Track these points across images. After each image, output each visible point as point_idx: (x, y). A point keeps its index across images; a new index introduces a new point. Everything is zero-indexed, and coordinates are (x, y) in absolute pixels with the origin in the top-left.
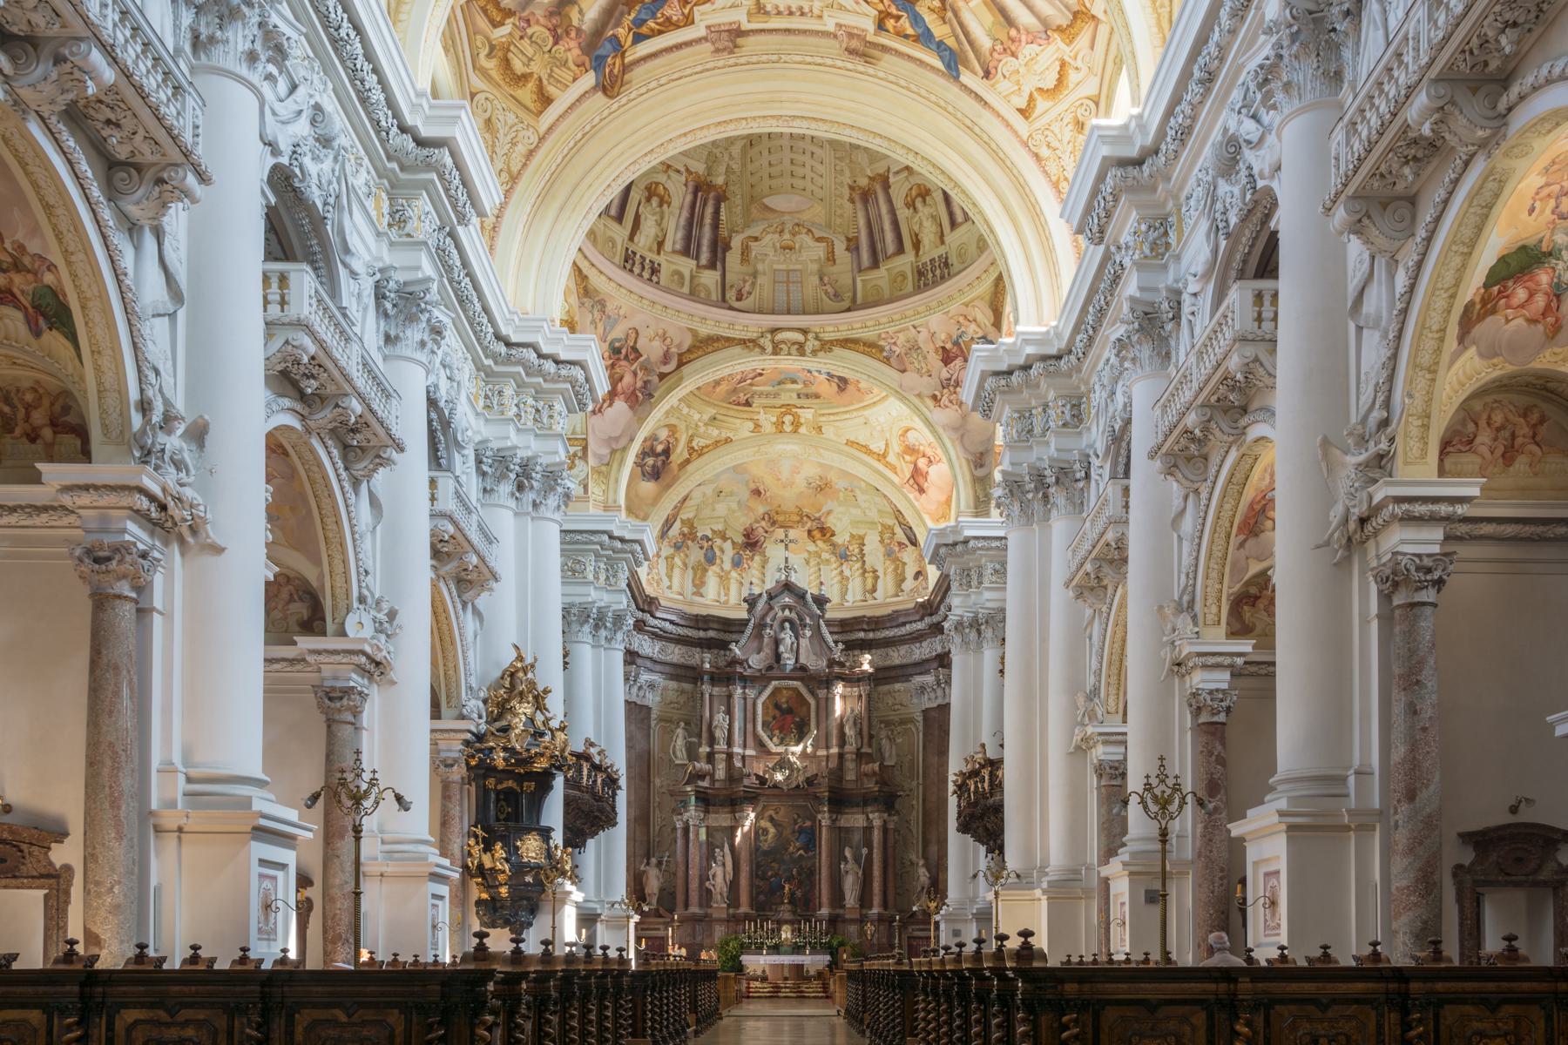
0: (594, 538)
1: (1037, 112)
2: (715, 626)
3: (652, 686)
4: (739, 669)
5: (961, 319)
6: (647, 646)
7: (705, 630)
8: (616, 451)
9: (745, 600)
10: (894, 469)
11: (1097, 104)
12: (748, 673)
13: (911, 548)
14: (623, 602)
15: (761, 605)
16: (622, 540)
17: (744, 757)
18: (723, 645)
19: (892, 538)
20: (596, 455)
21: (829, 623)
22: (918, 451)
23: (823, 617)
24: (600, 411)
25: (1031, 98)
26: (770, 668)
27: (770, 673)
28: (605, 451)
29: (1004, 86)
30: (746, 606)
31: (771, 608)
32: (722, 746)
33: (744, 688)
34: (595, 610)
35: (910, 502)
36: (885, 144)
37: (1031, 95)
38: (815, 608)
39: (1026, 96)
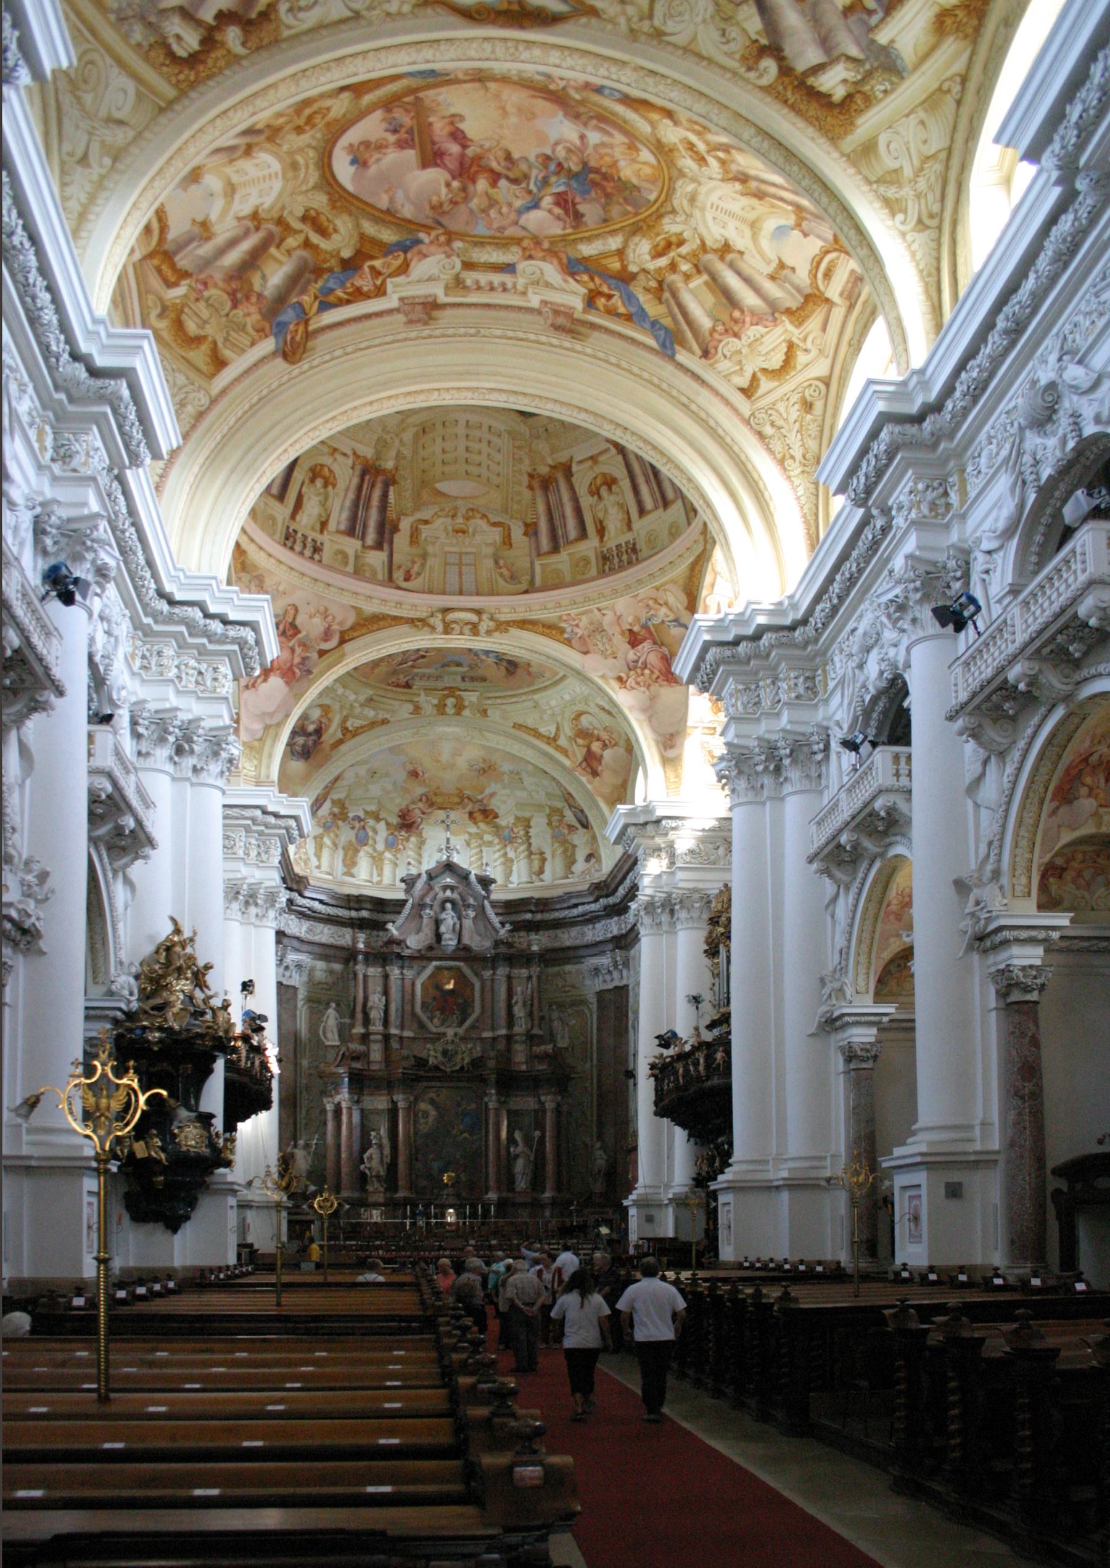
0: (248, 813)
1: (760, 392)
2: (368, 906)
3: (299, 966)
4: (397, 950)
5: (651, 603)
6: (297, 927)
7: (357, 910)
8: (271, 729)
9: (403, 880)
10: (565, 752)
11: (827, 385)
12: (407, 952)
13: (581, 831)
14: (272, 878)
15: (420, 885)
16: (276, 815)
17: (401, 1038)
18: (378, 926)
19: (561, 821)
20: (247, 729)
21: (494, 905)
22: (592, 735)
23: (488, 898)
24: (253, 686)
25: (754, 377)
26: (430, 948)
27: (429, 954)
28: (258, 726)
29: (724, 365)
30: (403, 885)
31: (431, 888)
32: (377, 1027)
33: (402, 967)
34: (245, 887)
35: (583, 786)
36: (591, 419)
37: (754, 375)
38: (479, 888)
39: (748, 375)
